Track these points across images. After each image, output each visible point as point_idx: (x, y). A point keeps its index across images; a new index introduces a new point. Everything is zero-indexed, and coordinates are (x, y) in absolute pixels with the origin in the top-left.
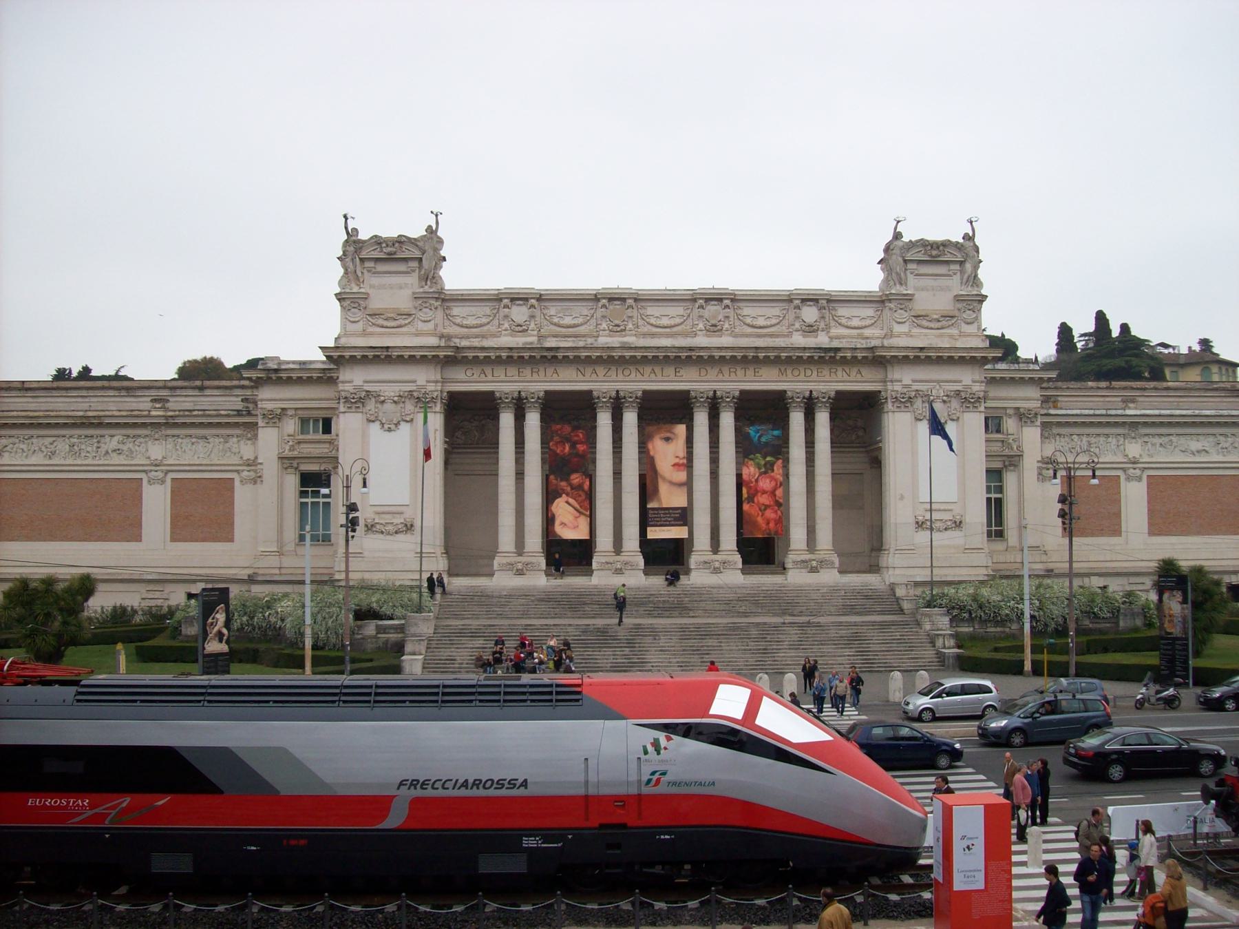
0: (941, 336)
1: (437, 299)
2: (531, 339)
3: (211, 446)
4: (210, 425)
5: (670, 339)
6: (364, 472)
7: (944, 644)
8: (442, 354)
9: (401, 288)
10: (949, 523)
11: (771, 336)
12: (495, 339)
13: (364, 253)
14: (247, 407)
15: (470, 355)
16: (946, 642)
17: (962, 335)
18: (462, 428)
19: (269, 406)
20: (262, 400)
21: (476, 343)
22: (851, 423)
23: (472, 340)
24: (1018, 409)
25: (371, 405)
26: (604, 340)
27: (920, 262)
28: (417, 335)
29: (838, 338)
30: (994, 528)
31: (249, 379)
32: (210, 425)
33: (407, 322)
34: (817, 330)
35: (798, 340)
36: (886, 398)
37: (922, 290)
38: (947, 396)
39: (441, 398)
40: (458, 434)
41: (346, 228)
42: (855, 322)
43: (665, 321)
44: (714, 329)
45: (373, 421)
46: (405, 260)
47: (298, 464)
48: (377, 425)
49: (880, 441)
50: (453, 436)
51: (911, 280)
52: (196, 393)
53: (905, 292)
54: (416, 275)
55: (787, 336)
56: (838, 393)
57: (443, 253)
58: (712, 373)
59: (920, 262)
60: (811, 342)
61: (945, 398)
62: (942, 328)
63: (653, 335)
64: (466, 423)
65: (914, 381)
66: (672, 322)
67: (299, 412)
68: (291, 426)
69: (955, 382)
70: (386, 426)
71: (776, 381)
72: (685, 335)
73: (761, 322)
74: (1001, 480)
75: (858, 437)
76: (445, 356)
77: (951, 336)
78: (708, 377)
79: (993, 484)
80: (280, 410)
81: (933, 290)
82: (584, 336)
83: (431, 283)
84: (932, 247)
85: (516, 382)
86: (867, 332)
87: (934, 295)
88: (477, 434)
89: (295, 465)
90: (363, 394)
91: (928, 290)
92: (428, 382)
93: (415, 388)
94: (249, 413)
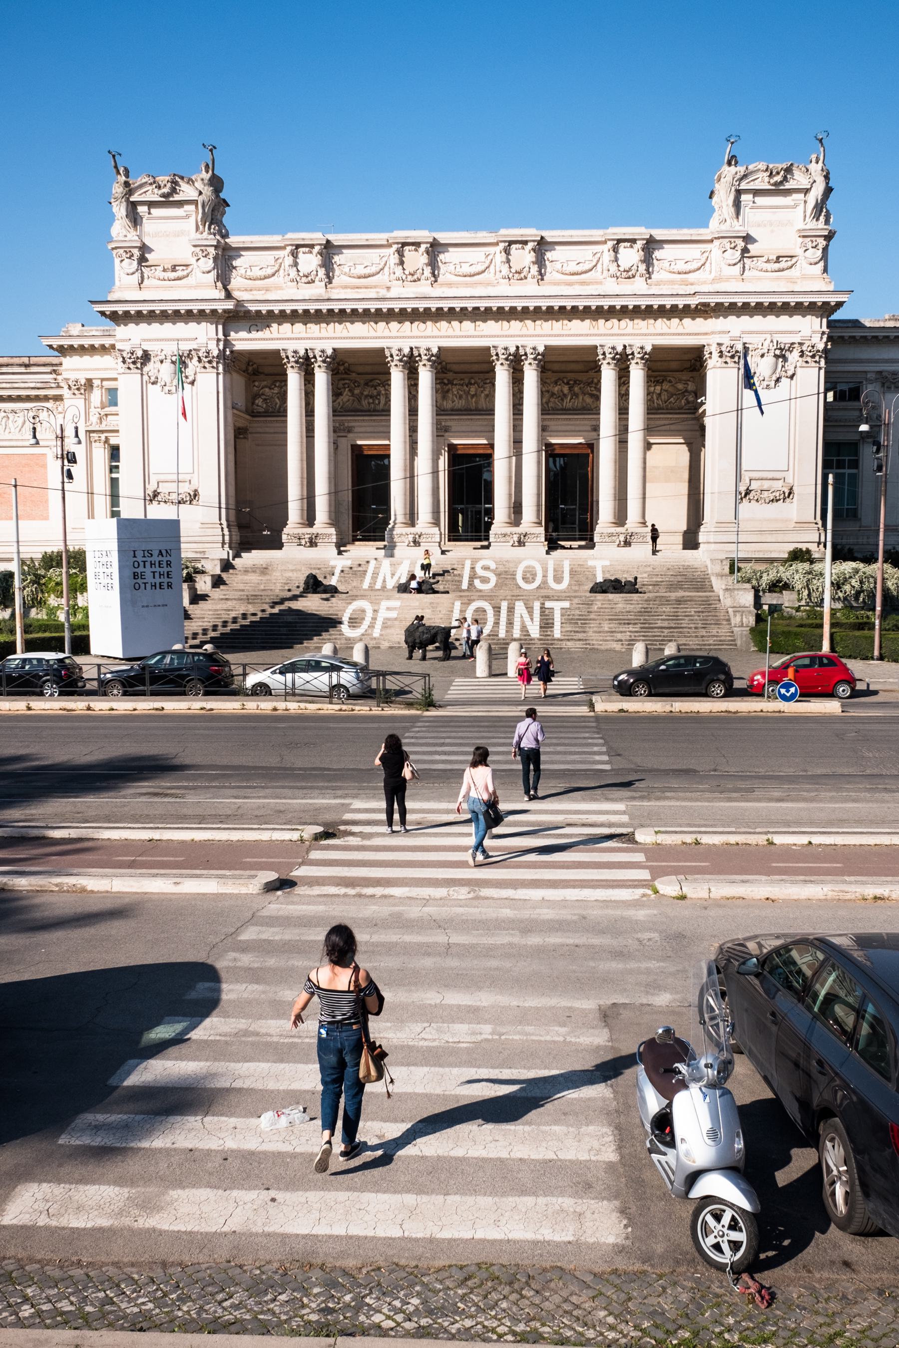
0: (778, 279)
1: (216, 247)
2: (318, 289)
3: (20, 421)
4: (19, 399)
5: (469, 289)
6: (76, 420)
7: (742, 621)
8: (220, 307)
9: (178, 236)
10: (777, 494)
11: (583, 283)
12: (279, 292)
13: (136, 195)
14: (55, 379)
15: (253, 308)
16: (744, 620)
17: (804, 277)
18: (263, 394)
19: (73, 376)
20: (66, 370)
21: (259, 296)
22: (680, 386)
23: (254, 292)
24: (880, 372)
25: (150, 367)
26: (393, 294)
27: (757, 193)
28: (196, 287)
29: (658, 284)
30: (846, 507)
31: (51, 347)
32: (19, 399)
33: (185, 273)
34: (634, 276)
35: (611, 286)
36: (711, 353)
37: (759, 226)
38: (780, 349)
39: (224, 359)
40: (259, 401)
41: (116, 167)
42: (680, 266)
43: (466, 269)
44: (521, 275)
45: (153, 383)
46: (180, 204)
47: (106, 437)
48: (157, 387)
49: (702, 404)
50: (253, 403)
51: (746, 211)
52: (23, 370)
53: (737, 228)
54: (192, 220)
55: (601, 283)
56: (655, 348)
57: (222, 195)
58: (515, 326)
59: (757, 193)
60: (627, 287)
61: (778, 352)
62: (783, 270)
63: (450, 285)
64: (267, 390)
65: (743, 332)
66: (473, 270)
67: (105, 383)
68: (96, 396)
69: (791, 332)
70: (166, 389)
71: (587, 335)
72: (488, 284)
73: (573, 267)
74: (856, 453)
75: (688, 402)
76: (225, 311)
77: (792, 281)
78: (511, 332)
79: (847, 458)
80: (83, 382)
81: (771, 225)
82: (375, 287)
83: (209, 229)
84: (771, 173)
85: (301, 339)
86: (691, 277)
87: (772, 231)
88: (277, 401)
89: (103, 438)
90: (140, 353)
91: (765, 226)
92: (209, 339)
93: (196, 347)
94: (59, 387)
